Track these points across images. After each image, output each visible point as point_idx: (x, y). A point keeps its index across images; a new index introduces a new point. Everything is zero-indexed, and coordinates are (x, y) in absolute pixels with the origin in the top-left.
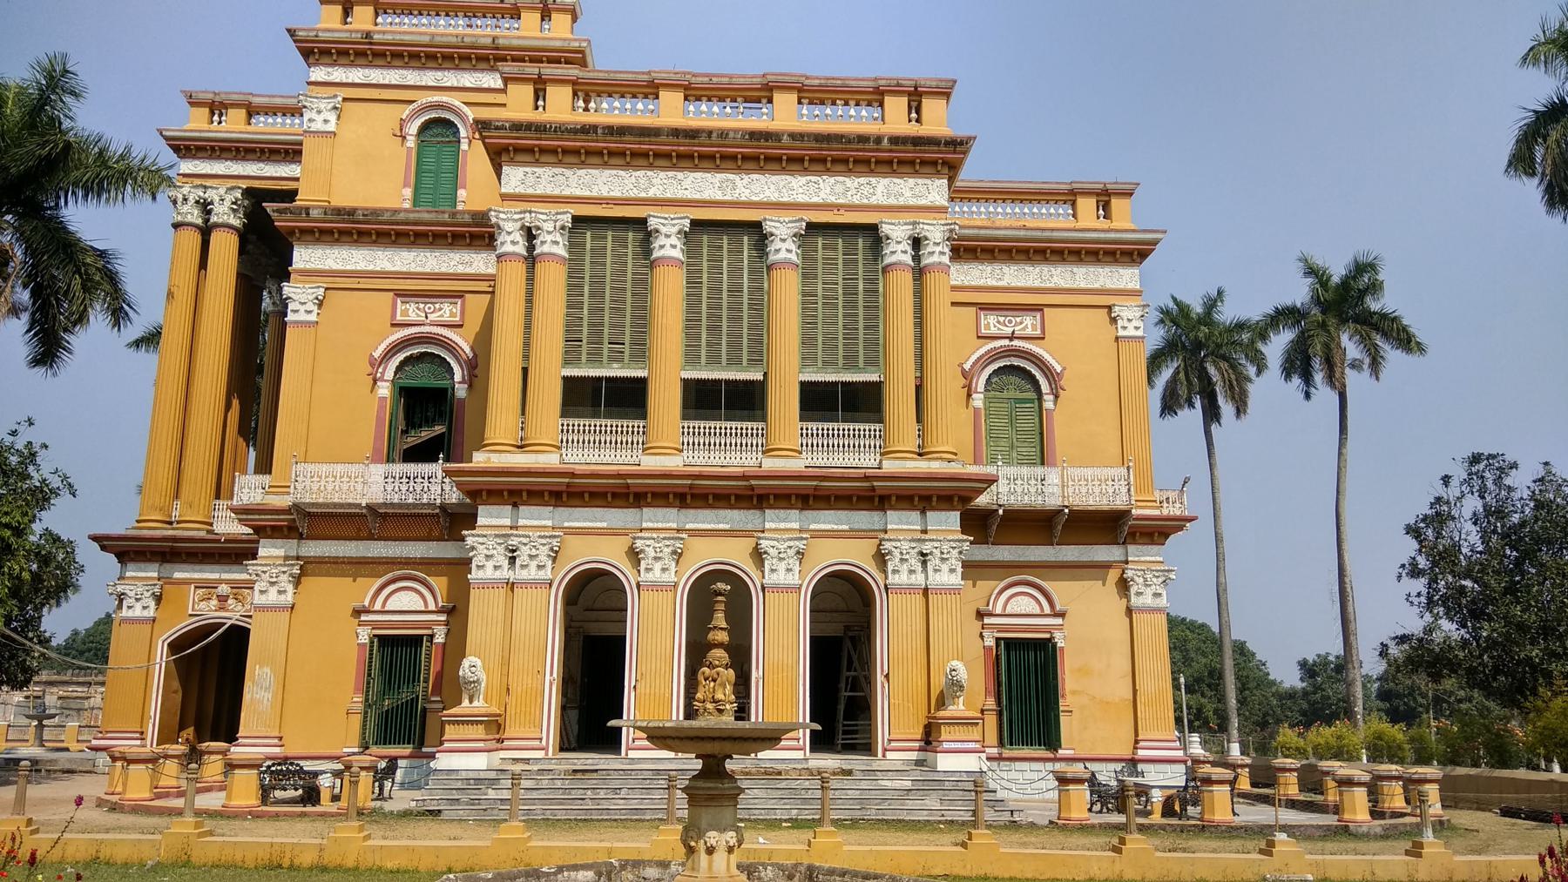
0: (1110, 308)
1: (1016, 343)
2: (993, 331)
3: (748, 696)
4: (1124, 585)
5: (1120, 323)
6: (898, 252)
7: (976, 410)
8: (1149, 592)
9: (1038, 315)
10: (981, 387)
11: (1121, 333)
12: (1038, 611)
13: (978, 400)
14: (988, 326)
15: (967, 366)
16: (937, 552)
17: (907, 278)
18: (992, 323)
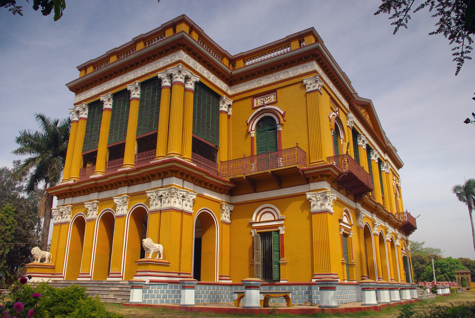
0: (302, 82)
1: (267, 107)
2: (259, 104)
3: (408, 271)
4: (308, 203)
5: (307, 86)
6: (166, 83)
7: (252, 138)
8: (319, 203)
9: (275, 93)
10: (254, 128)
11: (308, 90)
12: (273, 219)
13: (253, 134)
14: (257, 104)
15: (248, 122)
16: (164, 195)
17: (168, 90)
18: (258, 102)
